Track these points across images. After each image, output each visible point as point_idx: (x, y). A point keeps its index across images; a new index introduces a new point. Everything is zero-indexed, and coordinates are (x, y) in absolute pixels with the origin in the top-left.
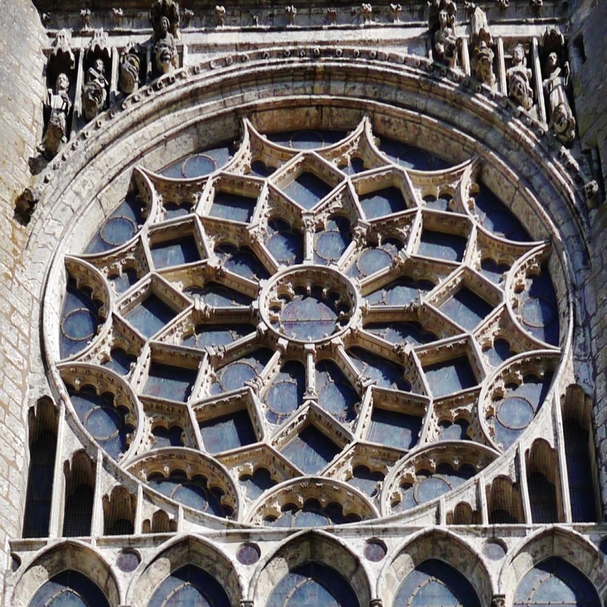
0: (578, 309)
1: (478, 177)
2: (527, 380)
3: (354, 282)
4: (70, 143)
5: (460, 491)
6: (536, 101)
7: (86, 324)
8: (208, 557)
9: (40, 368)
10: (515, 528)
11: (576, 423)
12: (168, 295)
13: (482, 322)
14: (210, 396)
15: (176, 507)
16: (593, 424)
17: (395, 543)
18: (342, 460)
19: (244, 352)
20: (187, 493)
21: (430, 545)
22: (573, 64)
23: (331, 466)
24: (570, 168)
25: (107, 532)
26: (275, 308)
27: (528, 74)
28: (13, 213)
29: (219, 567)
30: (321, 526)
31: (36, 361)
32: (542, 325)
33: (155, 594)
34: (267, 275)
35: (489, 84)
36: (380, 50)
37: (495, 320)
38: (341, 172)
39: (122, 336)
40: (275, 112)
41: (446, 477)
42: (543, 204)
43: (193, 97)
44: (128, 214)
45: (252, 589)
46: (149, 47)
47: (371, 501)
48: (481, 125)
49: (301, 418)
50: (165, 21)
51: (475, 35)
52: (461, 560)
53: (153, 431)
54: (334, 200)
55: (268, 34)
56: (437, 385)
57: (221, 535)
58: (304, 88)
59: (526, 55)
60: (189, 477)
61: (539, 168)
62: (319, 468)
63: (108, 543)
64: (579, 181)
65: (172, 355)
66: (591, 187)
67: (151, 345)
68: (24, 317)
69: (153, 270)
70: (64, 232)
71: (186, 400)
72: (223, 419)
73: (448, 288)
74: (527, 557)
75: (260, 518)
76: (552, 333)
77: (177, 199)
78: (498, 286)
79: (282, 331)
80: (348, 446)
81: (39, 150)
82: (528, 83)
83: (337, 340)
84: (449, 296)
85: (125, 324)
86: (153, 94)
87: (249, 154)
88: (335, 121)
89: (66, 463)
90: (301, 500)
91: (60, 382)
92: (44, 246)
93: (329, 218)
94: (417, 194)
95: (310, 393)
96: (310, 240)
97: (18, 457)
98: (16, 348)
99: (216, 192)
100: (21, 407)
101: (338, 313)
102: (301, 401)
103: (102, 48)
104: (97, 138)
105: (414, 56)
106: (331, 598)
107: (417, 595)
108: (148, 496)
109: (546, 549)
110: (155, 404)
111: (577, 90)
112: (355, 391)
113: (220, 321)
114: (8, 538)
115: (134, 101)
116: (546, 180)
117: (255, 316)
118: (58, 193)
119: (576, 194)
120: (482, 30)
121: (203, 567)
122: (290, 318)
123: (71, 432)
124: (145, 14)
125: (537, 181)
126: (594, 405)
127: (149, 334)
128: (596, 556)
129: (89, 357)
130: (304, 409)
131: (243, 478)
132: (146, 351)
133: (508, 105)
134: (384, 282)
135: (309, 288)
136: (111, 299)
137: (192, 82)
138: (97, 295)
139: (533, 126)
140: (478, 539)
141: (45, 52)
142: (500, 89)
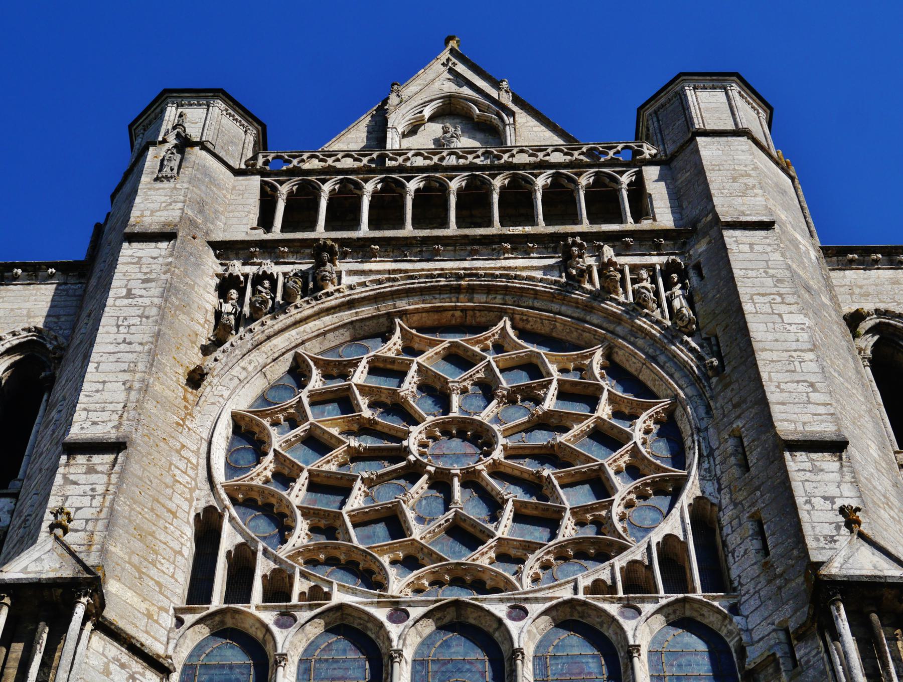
0: (703, 446)
1: (608, 356)
2: (655, 494)
3: (496, 427)
4: (239, 335)
5: (596, 572)
6: (659, 306)
7: (250, 457)
8: (360, 618)
9: (207, 486)
10: (648, 597)
11: (703, 519)
12: (326, 436)
13: (614, 454)
14: (363, 506)
15: (331, 583)
16: (719, 524)
17: (535, 609)
18: (486, 549)
19: (394, 475)
20: (340, 573)
21: (568, 610)
22: (693, 280)
23: (476, 554)
24: (692, 350)
25: (265, 600)
26: (423, 445)
27: (652, 288)
28: (185, 382)
29: (370, 625)
30: (466, 596)
31: (203, 481)
32: (669, 456)
33: (310, 645)
34: (416, 423)
35: (617, 295)
36: (518, 273)
37: (626, 453)
38: (484, 354)
39: (282, 464)
40: (424, 315)
41: (583, 562)
42: (668, 374)
43: (350, 304)
44: (290, 382)
45: (401, 641)
46: (311, 272)
47: (513, 579)
48: (610, 322)
49: (446, 521)
50: (326, 255)
51: (603, 263)
52: (599, 620)
53: (309, 530)
54: (478, 372)
55: (418, 264)
56: (571, 499)
57: (372, 603)
58: (450, 298)
59: (649, 276)
60: (343, 562)
61: (664, 350)
62: (464, 556)
63: (266, 608)
64: (700, 358)
65: (328, 477)
66: (712, 362)
67: (309, 471)
68: (193, 452)
69: (312, 419)
70: (231, 394)
71: (341, 508)
72: (376, 521)
73: (582, 431)
74: (660, 619)
75: (409, 591)
76: (679, 458)
77: (335, 372)
78: (628, 430)
79: (430, 461)
80: (491, 540)
81: (209, 339)
82: (652, 294)
83: (480, 467)
84: (583, 436)
85: (285, 457)
86: (314, 303)
87: (400, 342)
88: (478, 320)
89: (229, 552)
90: (447, 578)
91: (224, 496)
92: (213, 404)
93: (472, 385)
94: (553, 368)
95: (456, 504)
96: (456, 400)
97: (184, 548)
98: (185, 473)
99: (370, 368)
100: (188, 513)
101: (481, 449)
102: (447, 509)
103: (269, 273)
104: (263, 332)
105: (549, 277)
106: (476, 647)
107: (557, 645)
108: (303, 575)
109: (678, 612)
110: (312, 511)
111: (696, 298)
112: (497, 502)
113: (372, 454)
114: (172, 605)
115: (296, 307)
116: (669, 358)
117: (407, 451)
118: (227, 368)
119: (698, 367)
120: (609, 260)
121: (355, 626)
122: (437, 452)
123: (234, 531)
124: (308, 251)
125: (662, 359)
126: (720, 511)
127: (307, 463)
128: (725, 617)
129: (252, 479)
130: (450, 515)
131: (393, 563)
132: (305, 474)
133: (634, 308)
134: (523, 427)
135: (454, 432)
136: (273, 439)
137: (350, 295)
138: (261, 436)
139: (658, 322)
140: (613, 605)
141: (217, 275)
142: (626, 298)
